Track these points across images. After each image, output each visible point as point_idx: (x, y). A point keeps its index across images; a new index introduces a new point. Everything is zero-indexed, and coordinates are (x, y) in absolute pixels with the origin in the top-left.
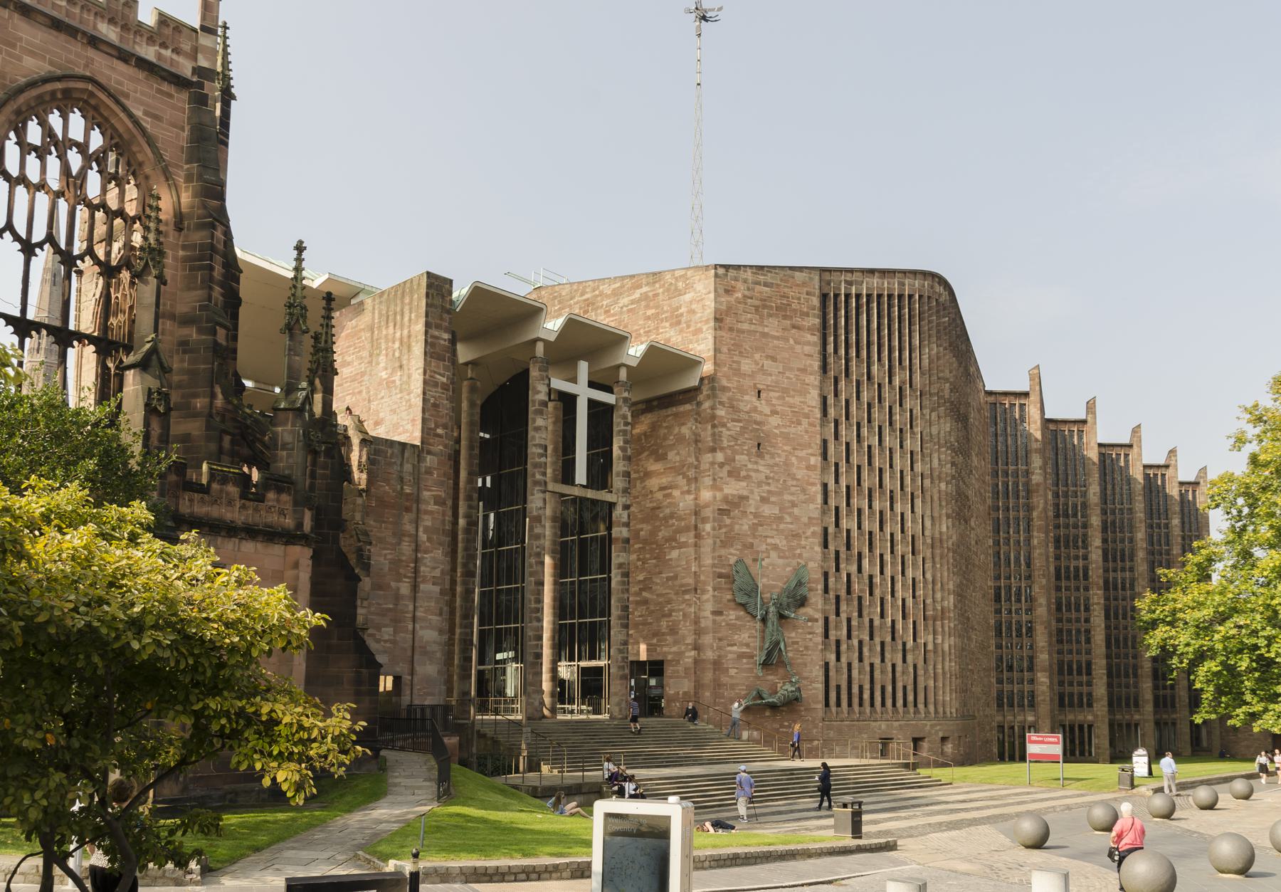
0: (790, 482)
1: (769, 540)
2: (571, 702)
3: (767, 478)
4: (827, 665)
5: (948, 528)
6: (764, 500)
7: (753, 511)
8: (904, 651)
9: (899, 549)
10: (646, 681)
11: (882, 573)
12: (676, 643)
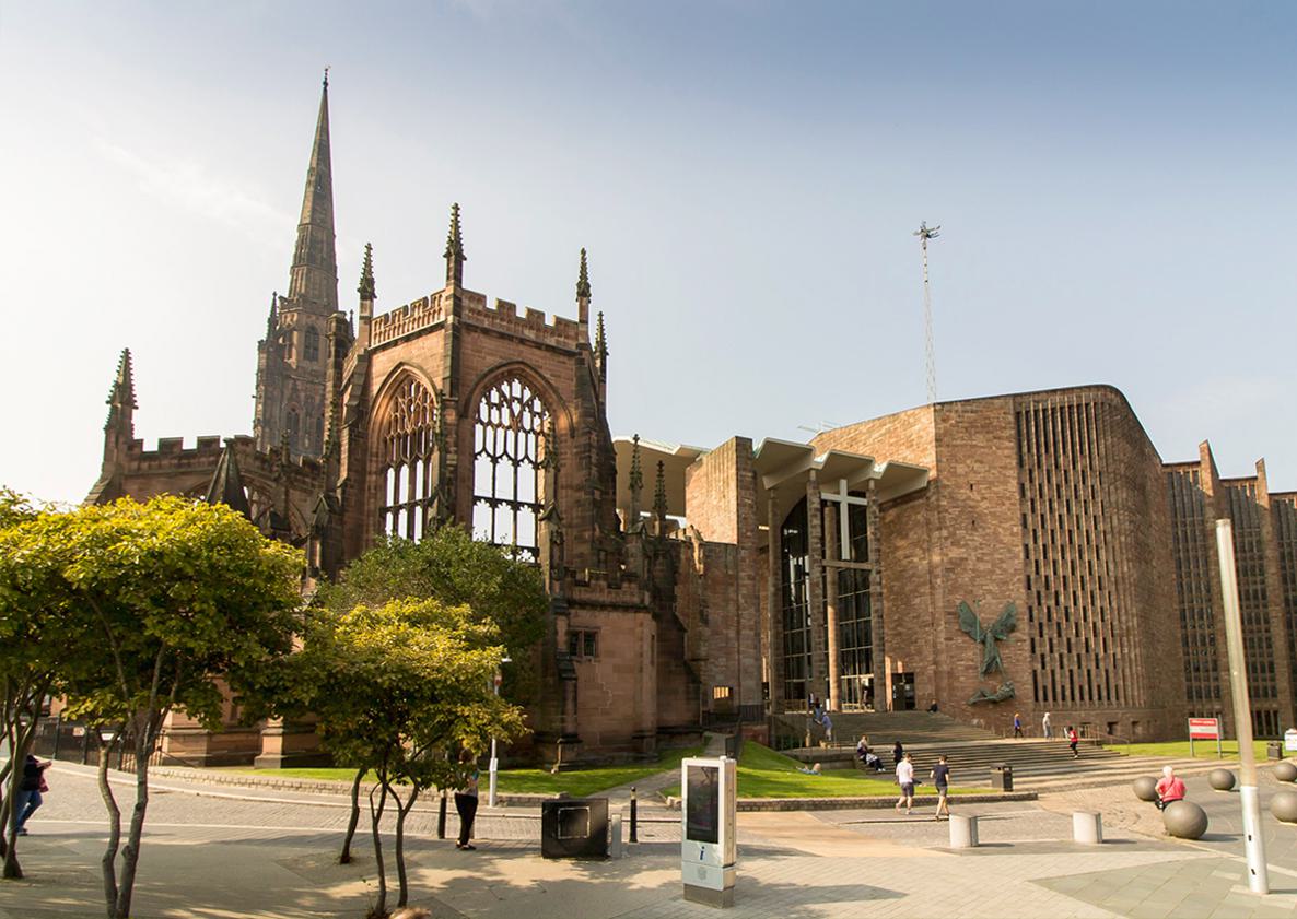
0: (998, 546)
1: (984, 587)
2: (856, 702)
3: (981, 544)
4: (1035, 672)
5: (1129, 568)
6: (978, 559)
7: (971, 567)
8: (1097, 660)
9: (1088, 587)
10: (903, 687)
11: (1075, 604)
12: (921, 660)
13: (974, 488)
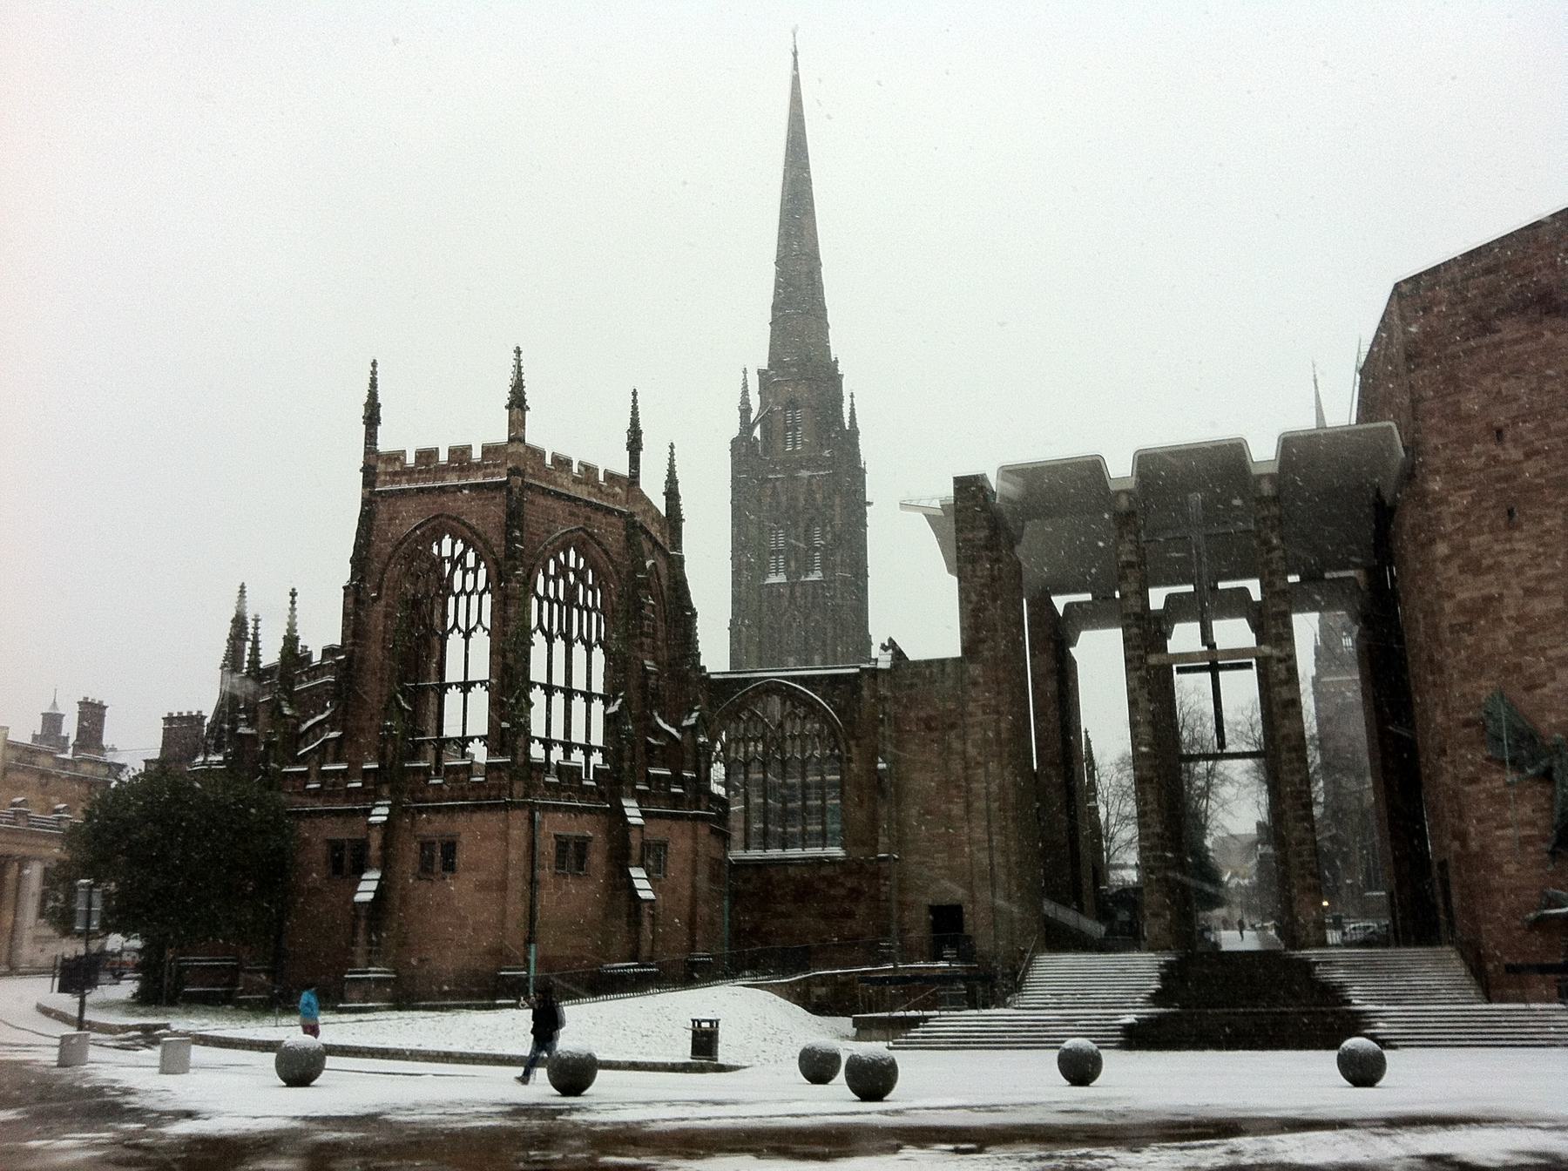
1: (1550, 653)
7: (1513, 613)
13: (1508, 435)
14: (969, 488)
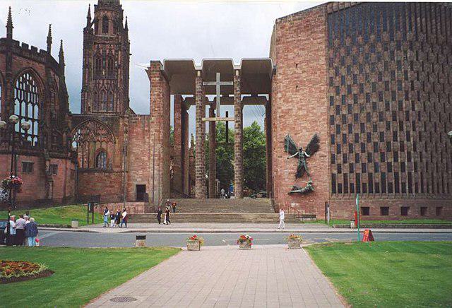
6: (299, 109)
13: (298, 66)
14: (154, 64)
